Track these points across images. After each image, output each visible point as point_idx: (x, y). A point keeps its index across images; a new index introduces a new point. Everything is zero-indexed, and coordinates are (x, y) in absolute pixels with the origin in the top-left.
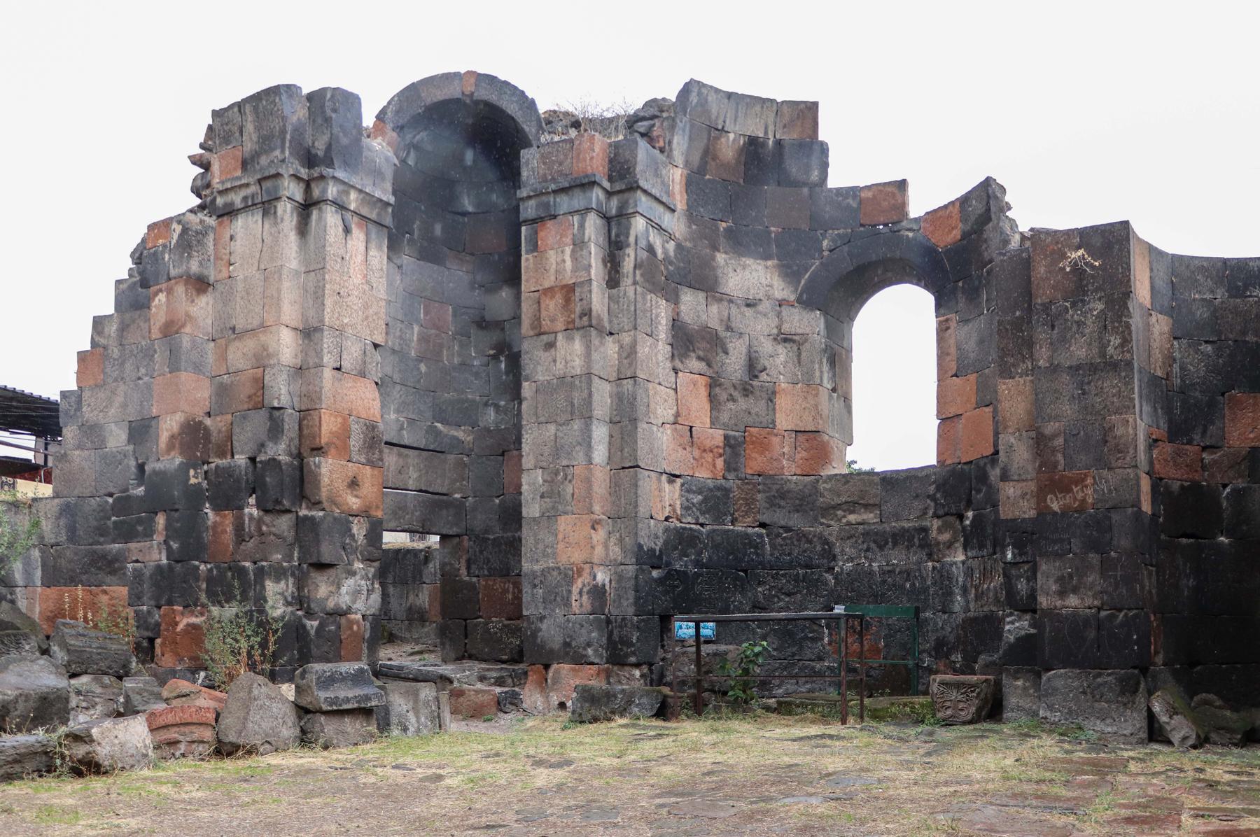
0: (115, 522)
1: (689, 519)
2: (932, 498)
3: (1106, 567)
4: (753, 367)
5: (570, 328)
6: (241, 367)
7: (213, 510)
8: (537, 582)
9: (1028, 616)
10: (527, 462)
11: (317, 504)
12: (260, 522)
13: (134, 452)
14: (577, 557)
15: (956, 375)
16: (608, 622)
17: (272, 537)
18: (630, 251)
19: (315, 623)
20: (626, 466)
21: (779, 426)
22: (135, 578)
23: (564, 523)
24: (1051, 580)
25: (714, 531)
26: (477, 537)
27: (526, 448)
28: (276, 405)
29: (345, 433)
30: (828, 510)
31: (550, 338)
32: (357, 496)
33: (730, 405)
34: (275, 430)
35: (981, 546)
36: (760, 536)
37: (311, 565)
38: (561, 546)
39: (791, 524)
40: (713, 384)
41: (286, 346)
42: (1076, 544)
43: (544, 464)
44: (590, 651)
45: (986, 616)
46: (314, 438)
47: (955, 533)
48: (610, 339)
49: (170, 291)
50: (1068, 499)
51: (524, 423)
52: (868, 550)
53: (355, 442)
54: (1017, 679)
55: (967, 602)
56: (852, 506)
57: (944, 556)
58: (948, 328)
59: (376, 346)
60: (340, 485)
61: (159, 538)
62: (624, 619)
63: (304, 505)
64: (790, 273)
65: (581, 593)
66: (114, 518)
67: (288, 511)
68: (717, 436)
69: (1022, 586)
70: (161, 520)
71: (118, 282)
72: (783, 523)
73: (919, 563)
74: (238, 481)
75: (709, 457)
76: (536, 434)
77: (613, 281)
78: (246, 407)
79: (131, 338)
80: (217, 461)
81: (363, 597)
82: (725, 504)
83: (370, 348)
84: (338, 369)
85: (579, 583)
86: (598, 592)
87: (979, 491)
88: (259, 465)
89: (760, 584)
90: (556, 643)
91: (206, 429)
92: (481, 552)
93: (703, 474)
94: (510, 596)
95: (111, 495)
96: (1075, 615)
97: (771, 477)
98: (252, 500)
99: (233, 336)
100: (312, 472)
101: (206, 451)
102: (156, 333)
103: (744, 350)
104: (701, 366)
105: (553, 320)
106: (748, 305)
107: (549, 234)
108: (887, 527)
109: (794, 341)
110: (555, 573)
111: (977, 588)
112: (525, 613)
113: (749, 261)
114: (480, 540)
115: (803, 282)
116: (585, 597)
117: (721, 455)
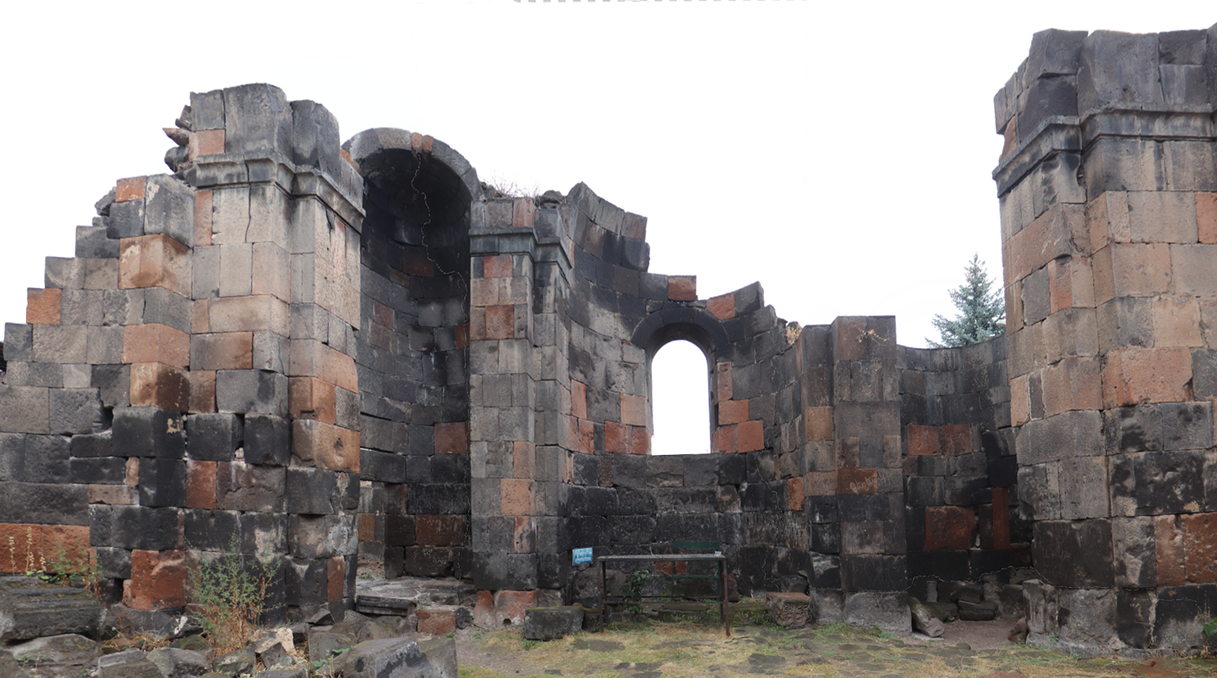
0: (73, 462)
3: (887, 529)
5: (510, 338)
7: (193, 459)
8: (484, 527)
13: (99, 395)
18: (551, 289)
20: (547, 443)
22: (99, 519)
26: (414, 485)
29: (331, 401)
31: (493, 343)
34: (265, 392)
35: (755, 505)
42: (868, 514)
46: (305, 402)
48: (535, 350)
49: (144, 246)
50: (863, 486)
55: (744, 538)
59: (354, 329)
61: (130, 482)
66: (72, 458)
69: (826, 538)
70: (133, 465)
71: (80, 229)
74: (223, 434)
76: (481, 414)
77: (538, 309)
79: (96, 282)
80: (196, 414)
83: (350, 330)
88: (248, 422)
90: (502, 576)
91: (186, 383)
95: (70, 435)
96: (869, 559)
100: (301, 431)
101: (185, 402)
102: (126, 282)
105: (496, 331)
107: (493, 265)
108: (688, 490)
114: (416, 486)
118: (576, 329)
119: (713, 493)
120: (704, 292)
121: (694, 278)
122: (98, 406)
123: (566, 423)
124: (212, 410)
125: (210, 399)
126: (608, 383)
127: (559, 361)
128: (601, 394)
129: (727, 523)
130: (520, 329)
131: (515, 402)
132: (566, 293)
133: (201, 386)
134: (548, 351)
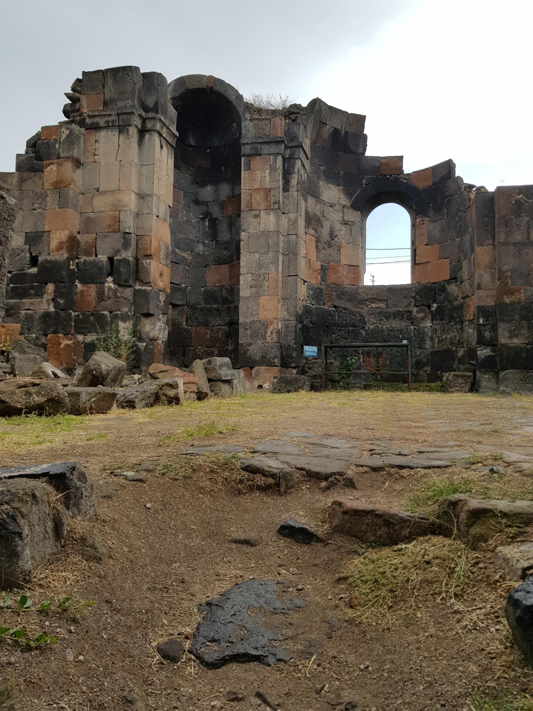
1: (308, 302)
2: (414, 298)
6: (102, 209)
9: (490, 347)
10: (242, 270)
11: (148, 283)
12: (115, 291)
13: (30, 249)
14: (270, 316)
15: (427, 245)
16: (281, 347)
17: (122, 299)
19: (144, 344)
20: (291, 275)
23: (263, 300)
24: (506, 331)
25: (317, 308)
28: (128, 231)
29: (158, 249)
30: (362, 302)
32: (162, 281)
33: (323, 251)
36: (334, 311)
37: (142, 314)
39: (346, 307)
40: (318, 241)
41: (131, 201)
43: (253, 272)
44: (276, 360)
45: (445, 350)
46: (146, 249)
47: (426, 313)
48: (284, 216)
51: (241, 251)
52: (381, 320)
53: (162, 255)
54: (486, 374)
56: (374, 300)
57: (420, 323)
58: (423, 224)
59: (170, 207)
60: (157, 275)
62: (289, 346)
63: (137, 284)
64: (348, 193)
65: (272, 333)
67: (131, 286)
68: (318, 265)
72: (343, 306)
73: (407, 326)
74: (101, 269)
75: (315, 273)
78: (106, 231)
80: (83, 258)
81: (162, 332)
82: (321, 296)
83: (168, 207)
84: (158, 216)
85: (271, 328)
86: (278, 332)
87: (441, 295)
88: (115, 261)
89: (334, 333)
91: (78, 241)
92: (193, 314)
93: (313, 282)
94: (208, 336)
97: (339, 285)
98: (110, 279)
99: (97, 193)
100: (144, 266)
101: (77, 252)
103: (329, 226)
104: (312, 232)
106: (331, 206)
108: (390, 310)
109: (349, 224)
110: (258, 323)
111: (439, 337)
112: (240, 342)
113: (332, 186)
115: (353, 198)
116: (274, 335)
117: (320, 274)
118: (310, 200)
119: (410, 312)
120: (408, 168)
121: (401, 158)
122: (28, 255)
123: (302, 263)
124: (94, 256)
125: (92, 250)
126: (332, 236)
127: (299, 222)
128: (328, 243)
129: (420, 336)
130: (275, 203)
131: (271, 249)
132: (305, 176)
133: (87, 242)
134: (292, 216)
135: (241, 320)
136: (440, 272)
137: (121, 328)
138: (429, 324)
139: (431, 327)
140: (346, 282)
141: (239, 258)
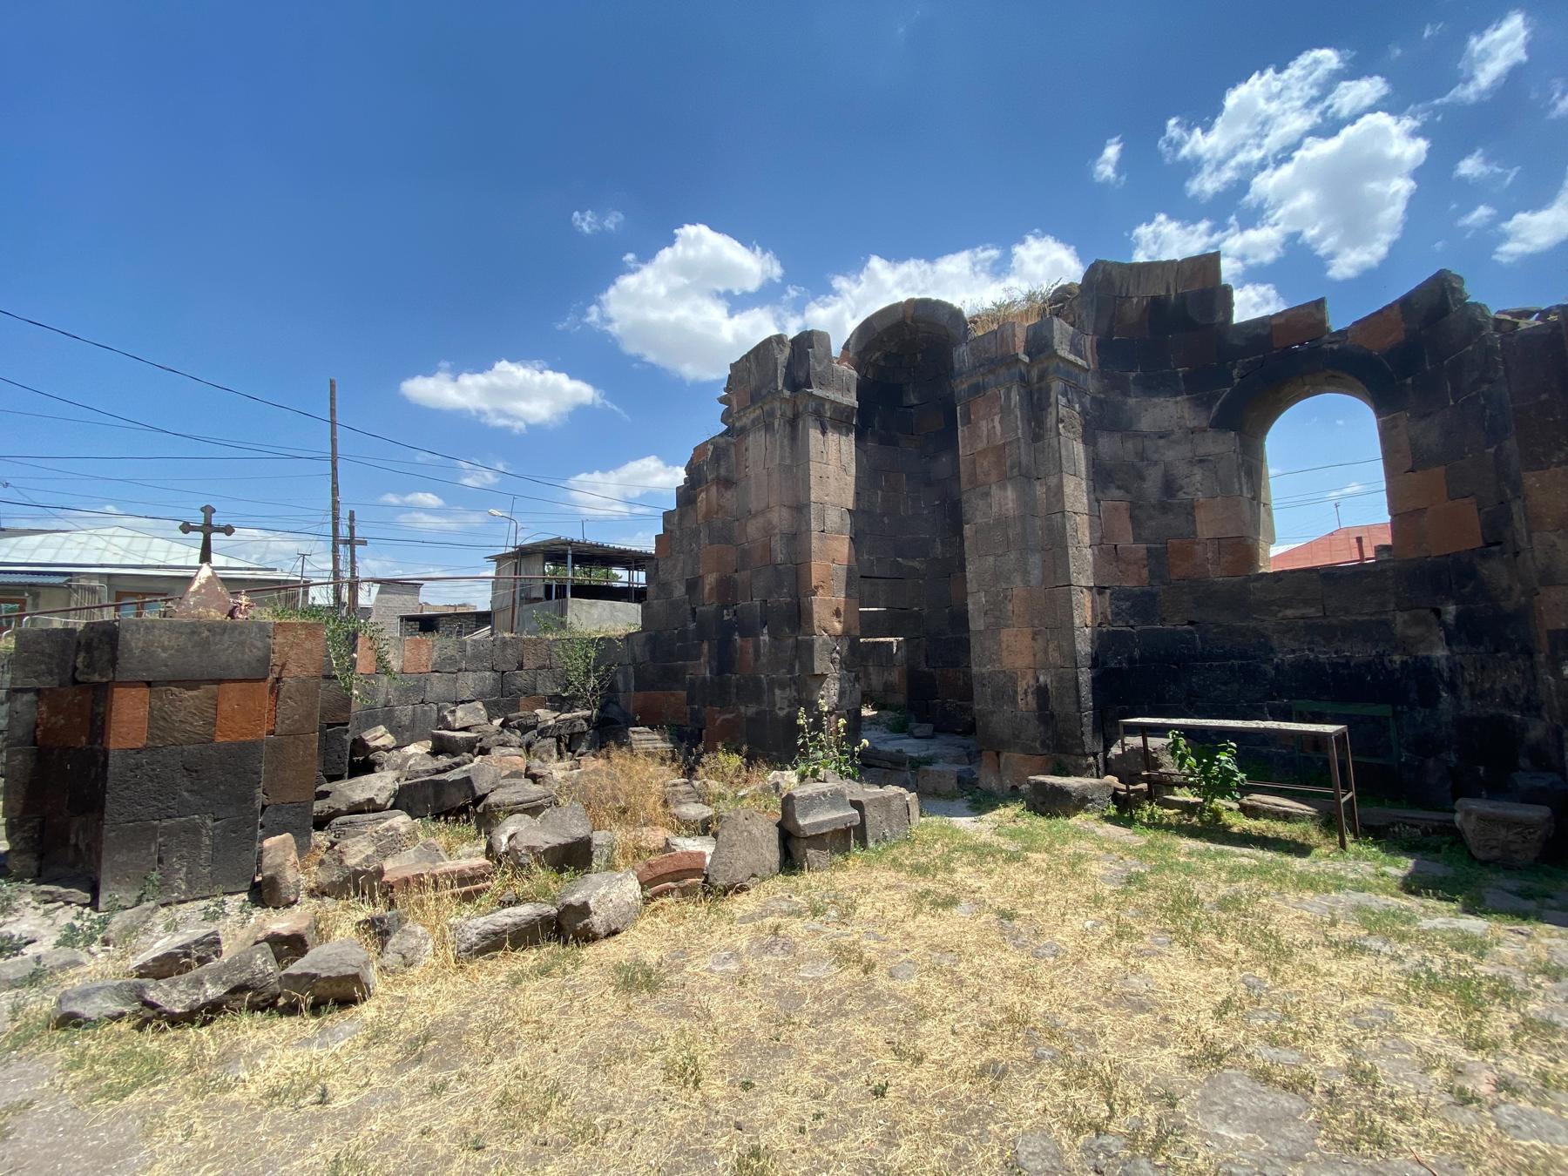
4: (1169, 486)
10: (971, 586)
21: (1200, 536)
23: (1006, 635)
27: (969, 575)
36: (1190, 632)
38: (1005, 654)
48: (1038, 483)
58: (1396, 427)
64: (1201, 403)
65: (1026, 693)
68: (1142, 548)
93: (1129, 584)
105: (987, 474)
115: (1214, 409)
116: (1030, 697)
120: (1338, 320)
135: (975, 669)
136: (1462, 531)
137: (777, 699)
138: (1440, 652)
139: (1448, 658)
140: (1217, 574)
141: (963, 568)
